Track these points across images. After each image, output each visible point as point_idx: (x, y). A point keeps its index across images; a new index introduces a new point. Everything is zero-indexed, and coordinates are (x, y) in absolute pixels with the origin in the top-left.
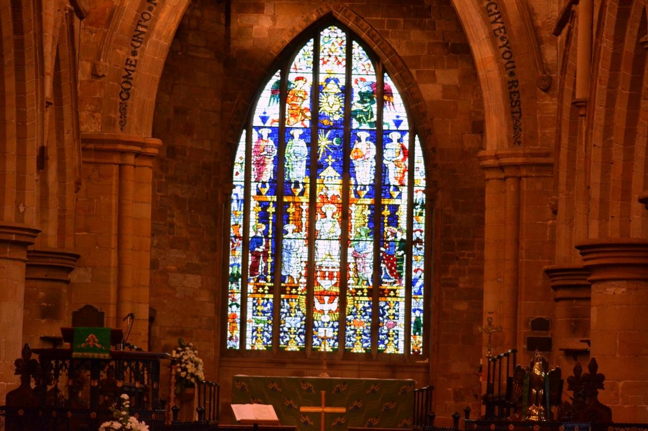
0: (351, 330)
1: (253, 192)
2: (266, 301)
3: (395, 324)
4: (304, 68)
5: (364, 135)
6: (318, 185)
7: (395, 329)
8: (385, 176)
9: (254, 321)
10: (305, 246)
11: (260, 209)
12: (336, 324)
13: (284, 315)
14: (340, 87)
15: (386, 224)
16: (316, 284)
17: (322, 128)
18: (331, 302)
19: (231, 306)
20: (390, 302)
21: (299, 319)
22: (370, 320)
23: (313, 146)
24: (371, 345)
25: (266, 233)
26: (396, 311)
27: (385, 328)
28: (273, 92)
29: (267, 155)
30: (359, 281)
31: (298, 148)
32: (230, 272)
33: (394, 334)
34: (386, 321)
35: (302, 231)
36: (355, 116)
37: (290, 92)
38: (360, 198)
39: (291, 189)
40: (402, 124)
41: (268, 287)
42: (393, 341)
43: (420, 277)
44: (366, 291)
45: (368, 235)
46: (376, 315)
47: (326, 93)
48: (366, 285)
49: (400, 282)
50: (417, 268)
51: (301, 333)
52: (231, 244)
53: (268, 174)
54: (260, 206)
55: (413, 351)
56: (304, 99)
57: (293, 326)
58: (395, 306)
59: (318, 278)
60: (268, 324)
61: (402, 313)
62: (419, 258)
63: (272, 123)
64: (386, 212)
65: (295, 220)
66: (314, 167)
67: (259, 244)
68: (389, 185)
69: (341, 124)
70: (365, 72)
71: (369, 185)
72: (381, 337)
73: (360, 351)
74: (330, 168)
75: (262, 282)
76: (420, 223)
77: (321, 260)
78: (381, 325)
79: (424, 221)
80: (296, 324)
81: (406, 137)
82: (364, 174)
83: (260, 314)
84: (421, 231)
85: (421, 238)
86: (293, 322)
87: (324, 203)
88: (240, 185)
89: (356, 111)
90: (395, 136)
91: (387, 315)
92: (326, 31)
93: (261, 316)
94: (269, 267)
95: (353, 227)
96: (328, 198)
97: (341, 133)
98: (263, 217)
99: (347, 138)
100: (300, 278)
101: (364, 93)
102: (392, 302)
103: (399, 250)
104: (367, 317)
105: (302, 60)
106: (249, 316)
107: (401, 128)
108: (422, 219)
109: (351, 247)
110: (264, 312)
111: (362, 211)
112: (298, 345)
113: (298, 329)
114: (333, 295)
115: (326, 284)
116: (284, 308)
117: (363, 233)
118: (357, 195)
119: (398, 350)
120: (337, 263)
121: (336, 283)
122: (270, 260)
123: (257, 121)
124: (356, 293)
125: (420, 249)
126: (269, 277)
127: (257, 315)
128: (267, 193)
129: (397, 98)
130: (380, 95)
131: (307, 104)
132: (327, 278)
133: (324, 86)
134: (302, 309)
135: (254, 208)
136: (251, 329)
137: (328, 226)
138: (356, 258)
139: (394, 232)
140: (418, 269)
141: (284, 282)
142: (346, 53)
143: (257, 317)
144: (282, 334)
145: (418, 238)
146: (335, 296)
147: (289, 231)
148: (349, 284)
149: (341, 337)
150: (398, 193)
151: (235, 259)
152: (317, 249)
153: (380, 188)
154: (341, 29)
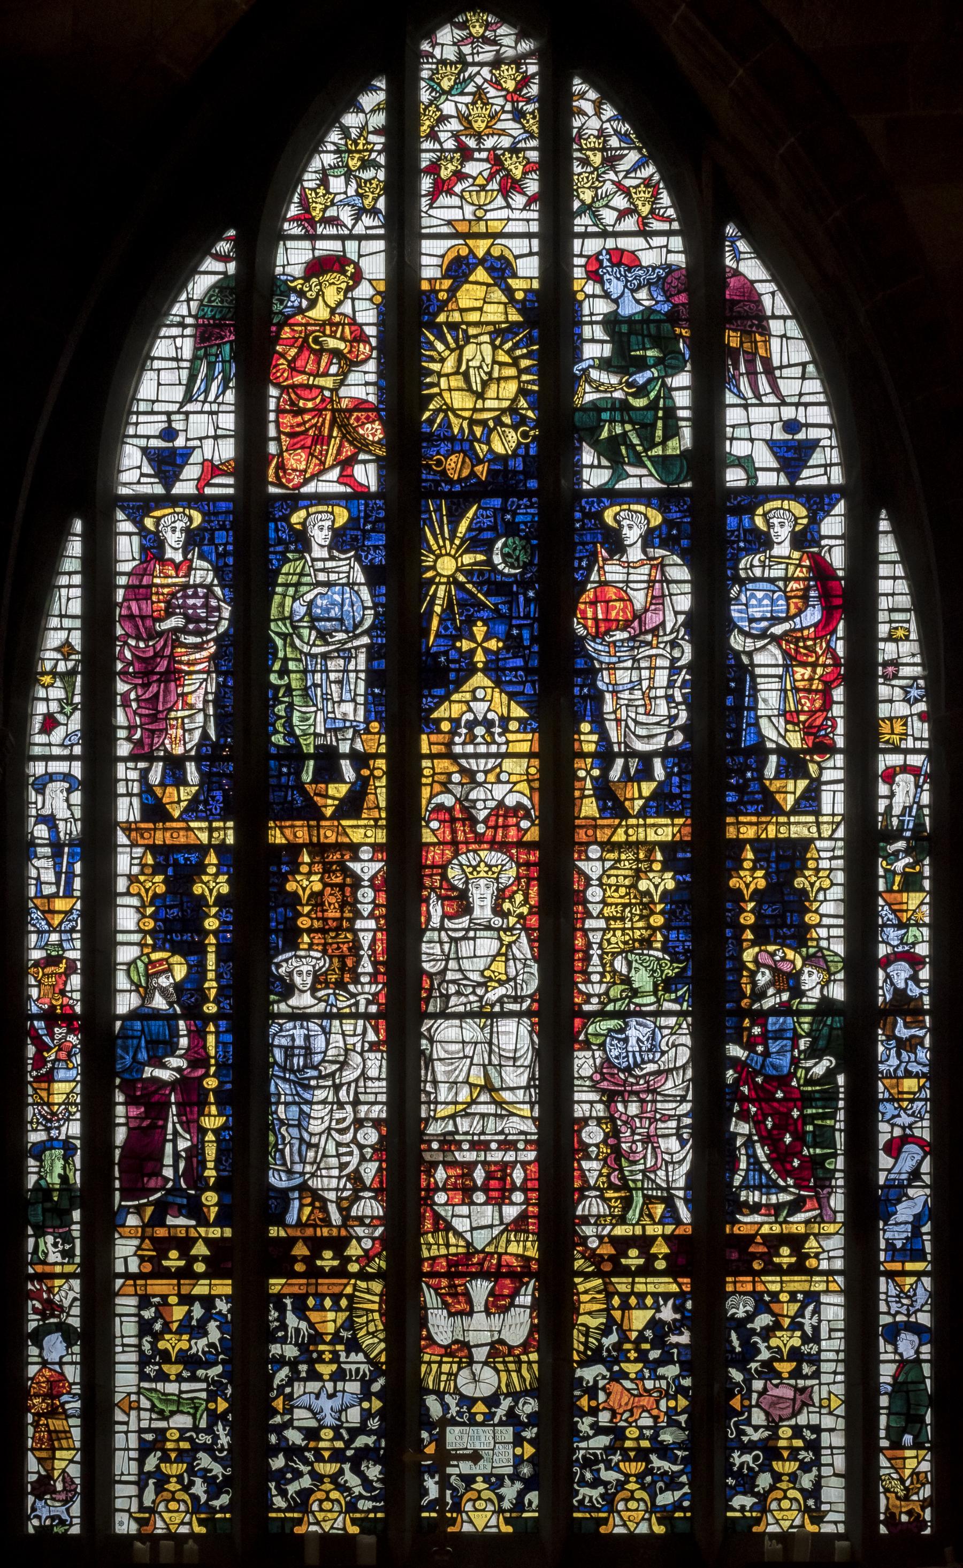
0: (599, 1430)
1: (127, 810)
2: (198, 1311)
3: (803, 1400)
4: (346, 215)
5: (634, 524)
6: (426, 763)
7: (802, 1420)
8: (739, 709)
9: (145, 1403)
10: (374, 1047)
11: (158, 884)
12: (529, 1407)
13: (284, 1373)
14: (520, 296)
15: (749, 935)
16: (428, 1225)
17: (437, 495)
18: (499, 1305)
19: (37, 1338)
20: (775, 1296)
21: (354, 1387)
22: (687, 1382)
23: (399, 576)
24: (693, 1496)
25: (189, 995)
26: (805, 1339)
27: (758, 1417)
28: (206, 335)
29: (184, 630)
30: (627, 1203)
31: (328, 586)
32: (32, 1180)
33: (798, 1443)
34: (758, 1385)
35: (356, 981)
36: (591, 434)
37: (286, 333)
38: (625, 815)
39: (300, 786)
40: (817, 458)
41: (208, 1242)
42: (793, 1478)
43: (915, 1174)
44: (661, 1248)
45: (667, 990)
46: (713, 1356)
47: (453, 327)
48: (662, 1222)
49: (822, 1203)
50: (897, 1132)
51: (365, 1454)
52: (31, 1050)
53: (193, 715)
54: (157, 869)
55: (892, 1519)
56: (349, 363)
57: (329, 1421)
58: (800, 1313)
59: (441, 1198)
60: (214, 1417)
61: (832, 1346)
62: (910, 1084)
63: (203, 481)
64: (750, 879)
65: (323, 931)
66: (408, 678)
67: (161, 1048)
68: (760, 751)
69: (527, 474)
70: (633, 224)
71: (666, 753)
72: (737, 1459)
73: (643, 1529)
74: (479, 679)
76: (910, 918)
77: (450, 1109)
78: (736, 1403)
79: (925, 914)
80: (344, 1409)
81: (833, 525)
82: (643, 703)
83: (173, 1370)
84: (915, 961)
85: (913, 991)
86: (326, 1405)
87: (454, 843)
88: (67, 777)
89: (595, 408)
90: (781, 522)
91: (765, 1355)
92: (446, 35)
93: (180, 1379)
94: (211, 1152)
95: (595, 952)
96: (473, 821)
97: (526, 514)
98: (176, 924)
99: (562, 538)
100: (356, 1198)
101: (630, 320)
102: (784, 1297)
103: (815, 1053)
104: (671, 1371)
105: (337, 179)
106: (126, 1380)
107: (811, 477)
108: (917, 903)
109: (587, 1045)
110: (190, 1361)
111: (638, 874)
112: (351, 1507)
113: (354, 1433)
114: (512, 1275)
115: (477, 1223)
116: (283, 1340)
117: (642, 979)
118: (612, 804)
119: (818, 1518)
120: (523, 1123)
121: (522, 1218)
122: (213, 1121)
123: (133, 472)
124: (614, 1259)
125: (910, 1045)
126: (210, 1198)
127: (163, 1377)
128: (193, 809)
129: (788, 345)
130: (703, 326)
131: (361, 386)
132: (480, 1197)
133: (443, 296)
134: (367, 1342)
135: (132, 879)
136: (133, 1442)
137: (480, 946)
138: (610, 1098)
139: (786, 967)
140: (906, 1139)
141: (281, 1223)
142: (542, 136)
143: (160, 1386)
144: (278, 1462)
145: (900, 994)
146: (518, 1277)
147: (298, 980)
148: (585, 1220)
149: (553, 1465)
150: (802, 784)
151: (49, 1121)
152: (430, 1061)
153: (716, 763)
154: (512, 25)
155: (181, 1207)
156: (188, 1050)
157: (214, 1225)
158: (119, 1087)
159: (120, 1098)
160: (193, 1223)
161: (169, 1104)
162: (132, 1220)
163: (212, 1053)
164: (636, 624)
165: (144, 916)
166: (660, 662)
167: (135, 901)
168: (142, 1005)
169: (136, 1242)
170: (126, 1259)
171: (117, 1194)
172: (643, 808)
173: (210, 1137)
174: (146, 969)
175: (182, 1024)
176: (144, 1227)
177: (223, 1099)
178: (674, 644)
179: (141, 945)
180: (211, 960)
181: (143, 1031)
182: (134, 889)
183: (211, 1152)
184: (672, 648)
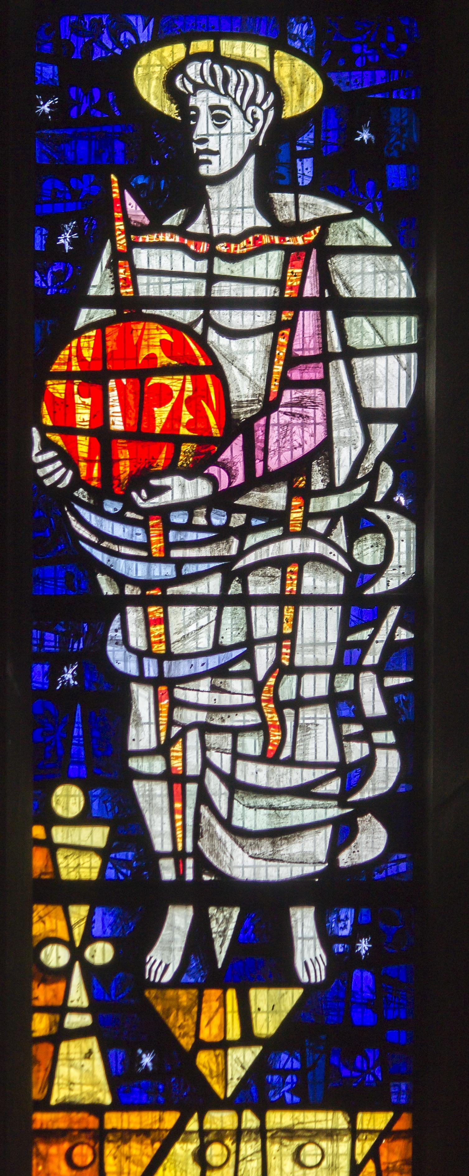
164: (235, 452)
166: (314, 581)
172: (256, 1073)
178: (360, 521)
184: (353, 537)
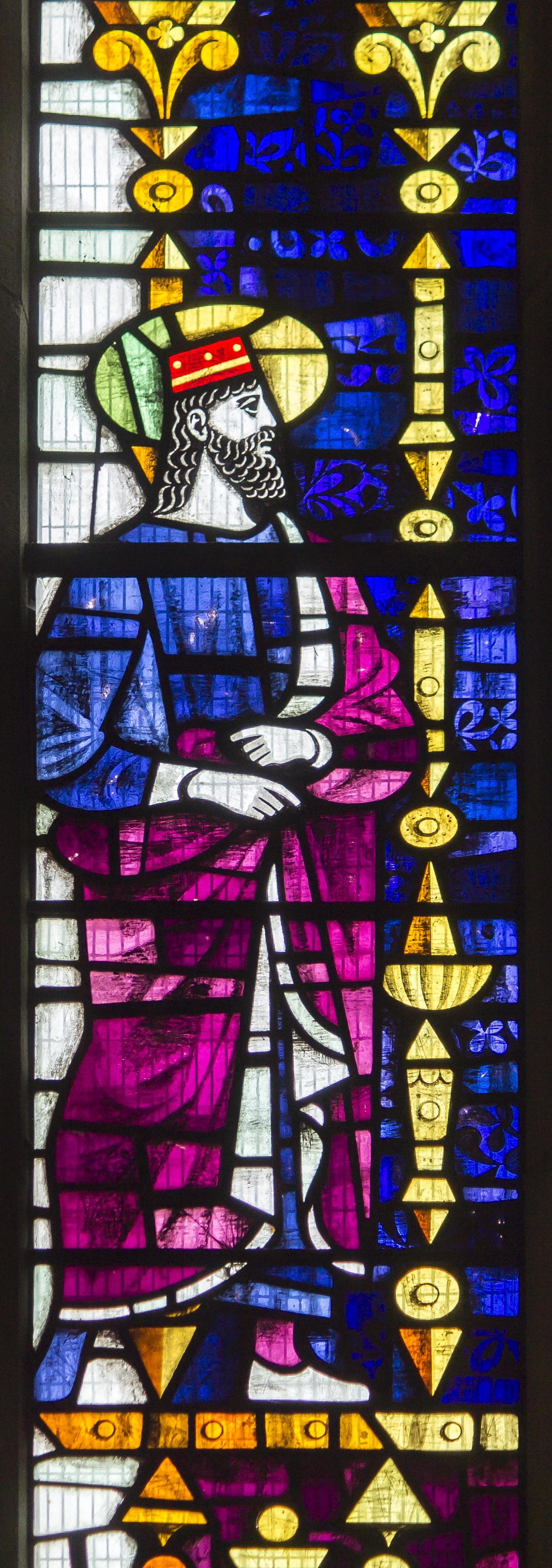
25: (334, 479)
41: (419, 1469)
75: (299, 1393)
94: (431, 1103)
122: (438, 982)
126: (430, 1293)
155: (306, 1327)
156: (332, 694)
157: (450, 1399)
158: (46, 842)
159: (53, 884)
160: (359, 1393)
161: (257, 913)
162: (107, 1383)
163: (435, 708)
165: (152, 161)
167: (118, 101)
168: (145, 516)
169: (123, 1473)
170: (77, 1542)
171: (43, 1275)
173: (428, 1044)
174: (164, 373)
175: (309, 592)
176: (153, 1408)
177: (477, 890)
179: (138, 273)
180: (430, 331)
181: (146, 618)
182: (111, 52)
183: (431, 1103)
